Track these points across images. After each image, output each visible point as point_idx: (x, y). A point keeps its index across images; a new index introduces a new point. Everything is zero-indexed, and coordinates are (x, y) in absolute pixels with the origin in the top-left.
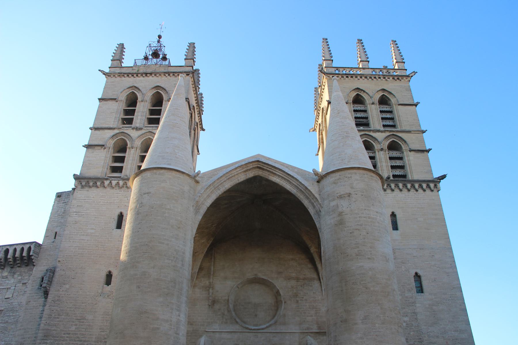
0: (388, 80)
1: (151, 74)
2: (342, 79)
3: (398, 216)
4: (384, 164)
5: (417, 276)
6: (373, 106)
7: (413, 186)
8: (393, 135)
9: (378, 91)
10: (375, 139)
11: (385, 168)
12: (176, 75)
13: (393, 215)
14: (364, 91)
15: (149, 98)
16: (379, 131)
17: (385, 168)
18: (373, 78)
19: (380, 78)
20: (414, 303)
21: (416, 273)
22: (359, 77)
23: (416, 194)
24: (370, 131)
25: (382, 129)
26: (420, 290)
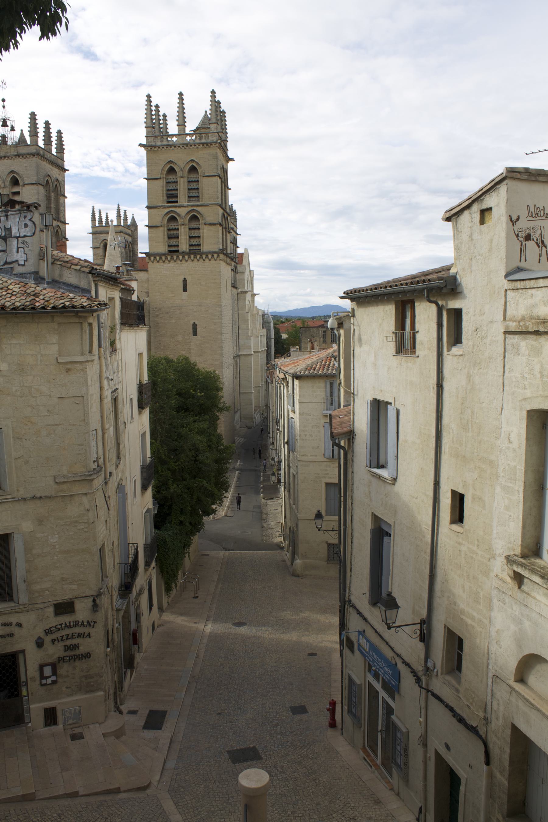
0: (199, 147)
1: (5, 157)
2: (159, 149)
3: (188, 282)
4: (183, 237)
5: (195, 326)
6: (182, 179)
7: (201, 257)
8: (193, 209)
9: (187, 163)
10: (179, 215)
11: (183, 241)
12: (25, 156)
13: (185, 280)
14: (176, 164)
15: (8, 184)
16: (183, 206)
17: (183, 241)
18: (185, 147)
19: (191, 146)
20: (190, 342)
21: (194, 323)
22: (173, 147)
23: (203, 263)
24: (176, 207)
25: (186, 204)
26: (195, 333)
